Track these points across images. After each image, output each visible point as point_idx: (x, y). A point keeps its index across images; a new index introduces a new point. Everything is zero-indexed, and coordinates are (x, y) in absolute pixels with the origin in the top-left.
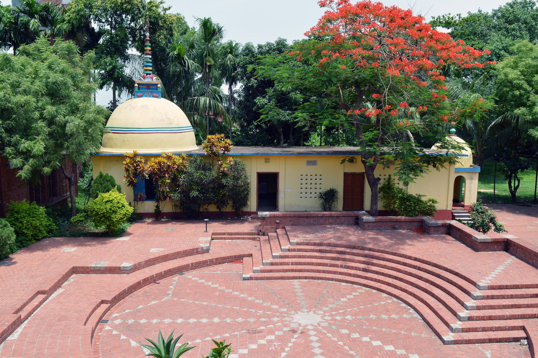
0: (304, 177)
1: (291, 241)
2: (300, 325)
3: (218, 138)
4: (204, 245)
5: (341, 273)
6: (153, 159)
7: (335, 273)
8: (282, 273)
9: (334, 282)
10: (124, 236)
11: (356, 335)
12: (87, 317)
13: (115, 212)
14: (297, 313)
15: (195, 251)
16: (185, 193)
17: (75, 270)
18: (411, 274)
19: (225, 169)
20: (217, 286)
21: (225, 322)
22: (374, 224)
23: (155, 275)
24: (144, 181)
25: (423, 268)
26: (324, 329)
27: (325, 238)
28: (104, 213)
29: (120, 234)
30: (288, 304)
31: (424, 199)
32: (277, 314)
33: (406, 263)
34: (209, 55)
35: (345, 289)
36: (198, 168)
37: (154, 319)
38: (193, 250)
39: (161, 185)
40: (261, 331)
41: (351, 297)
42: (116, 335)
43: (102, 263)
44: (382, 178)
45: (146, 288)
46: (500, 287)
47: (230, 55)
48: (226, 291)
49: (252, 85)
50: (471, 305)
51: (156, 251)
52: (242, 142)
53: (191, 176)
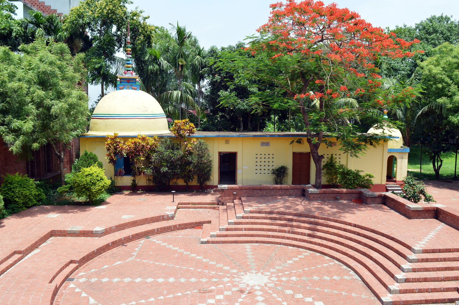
0: (259, 156)
1: (245, 210)
2: (248, 285)
3: (184, 122)
4: (170, 213)
5: (288, 238)
6: (130, 140)
7: (283, 238)
8: (236, 238)
9: (282, 246)
10: (103, 205)
11: (299, 296)
12: (53, 275)
13: (94, 184)
14: (246, 274)
15: (161, 218)
16: (157, 169)
17: (53, 234)
18: (351, 239)
19: (190, 148)
20: (177, 248)
21: (180, 281)
22: (319, 196)
23: (123, 239)
24: (123, 159)
25: (362, 234)
26: (270, 290)
27: (276, 207)
28: (84, 184)
29: (99, 203)
30: (239, 266)
31: (362, 174)
32: (228, 275)
33: (347, 229)
34: (182, 57)
35: (292, 252)
36: (168, 148)
37: (115, 278)
38: (160, 217)
39: (136, 162)
40: (211, 291)
41: (297, 259)
42: (78, 292)
43: (78, 227)
44: (325, 156)
45: (115, 250)
46: (434, 251)
47: (198, 57)
48: (185, 253)
49: (217, 80)
50: (407, 268)
51: (126, 218)
52: (208, 128)
53: (161, 155)
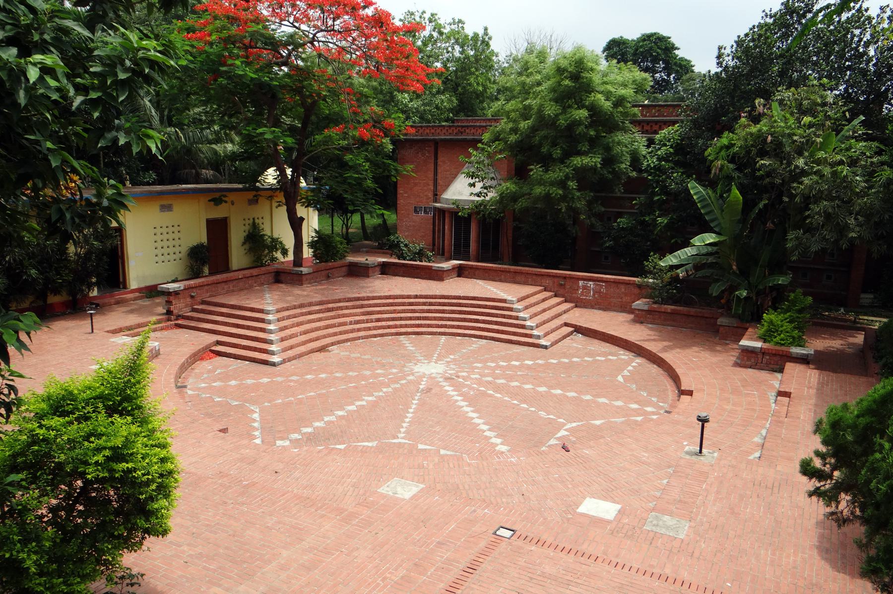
7: (352, 331)
